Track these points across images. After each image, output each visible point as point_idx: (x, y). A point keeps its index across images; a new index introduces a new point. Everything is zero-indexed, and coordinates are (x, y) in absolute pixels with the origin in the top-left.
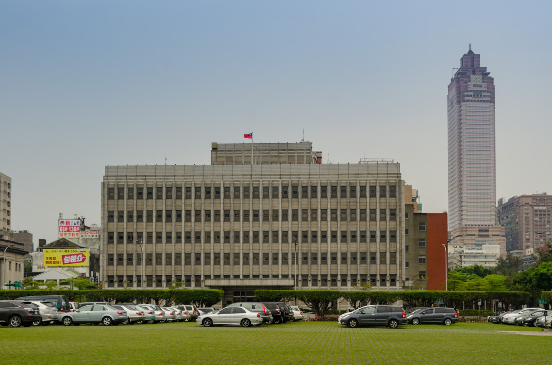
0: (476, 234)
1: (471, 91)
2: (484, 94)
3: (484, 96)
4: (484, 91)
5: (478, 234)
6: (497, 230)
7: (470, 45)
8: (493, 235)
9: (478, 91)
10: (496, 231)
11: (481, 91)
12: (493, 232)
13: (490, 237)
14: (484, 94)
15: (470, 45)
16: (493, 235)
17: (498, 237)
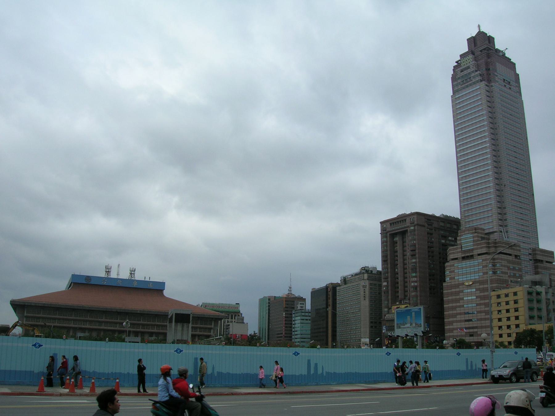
0: (459, 256)
1: (459, 78)
2: (473, 75)
3: (474, 77)
4: (473, 72)
5: (460, 256)
6: (482, 246)
7: (479, 26)
8: (479, 255)
9: (466, 75)
10: (482, 248)
11: (469, 73)
12: (478, 250)
13: (475, 257)
14: (473, 75)
15: (479, 26)
16: (479, 255)
17: (484, 257)
